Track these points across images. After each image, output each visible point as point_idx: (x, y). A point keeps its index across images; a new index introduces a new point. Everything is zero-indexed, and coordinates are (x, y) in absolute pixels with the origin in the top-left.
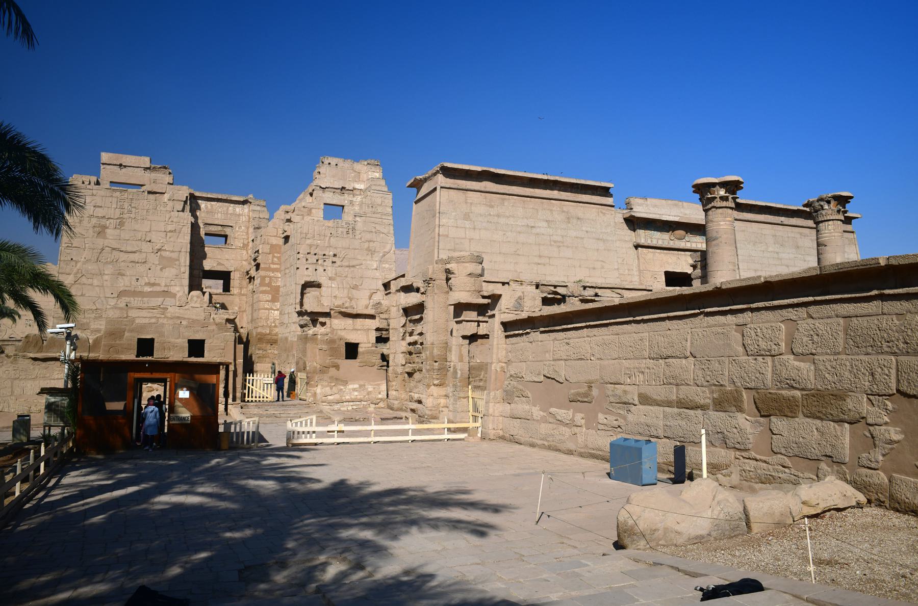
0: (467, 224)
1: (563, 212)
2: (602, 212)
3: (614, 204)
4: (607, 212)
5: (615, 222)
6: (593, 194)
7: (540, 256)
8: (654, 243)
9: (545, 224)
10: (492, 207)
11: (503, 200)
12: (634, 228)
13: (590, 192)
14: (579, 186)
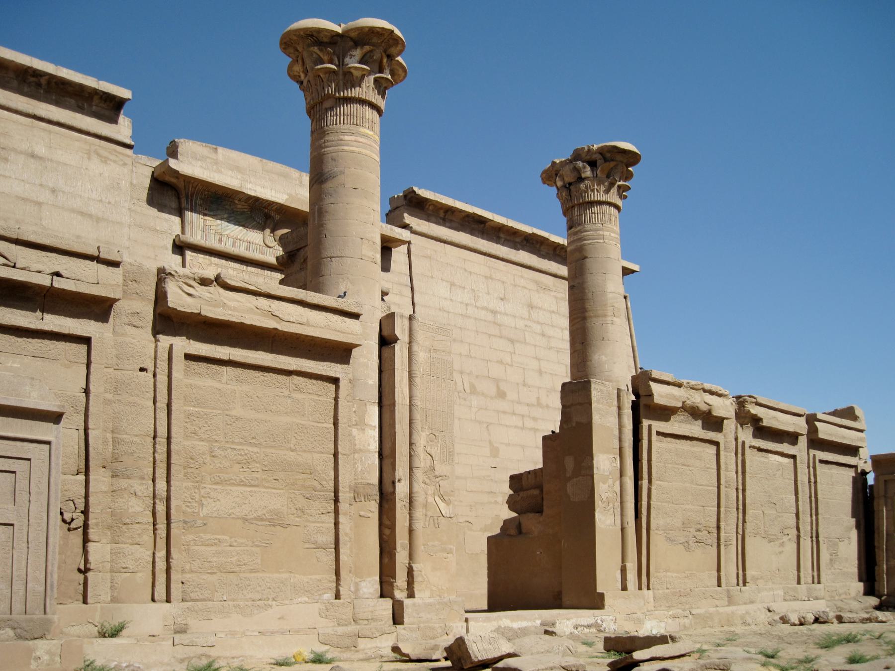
2: (98, 154)
3: (133, 143)
4: (112, 157)
5: (131, 184)
6: (80, 109)
8: (227, 247)
12: (180, 203)
13: (73, 102)
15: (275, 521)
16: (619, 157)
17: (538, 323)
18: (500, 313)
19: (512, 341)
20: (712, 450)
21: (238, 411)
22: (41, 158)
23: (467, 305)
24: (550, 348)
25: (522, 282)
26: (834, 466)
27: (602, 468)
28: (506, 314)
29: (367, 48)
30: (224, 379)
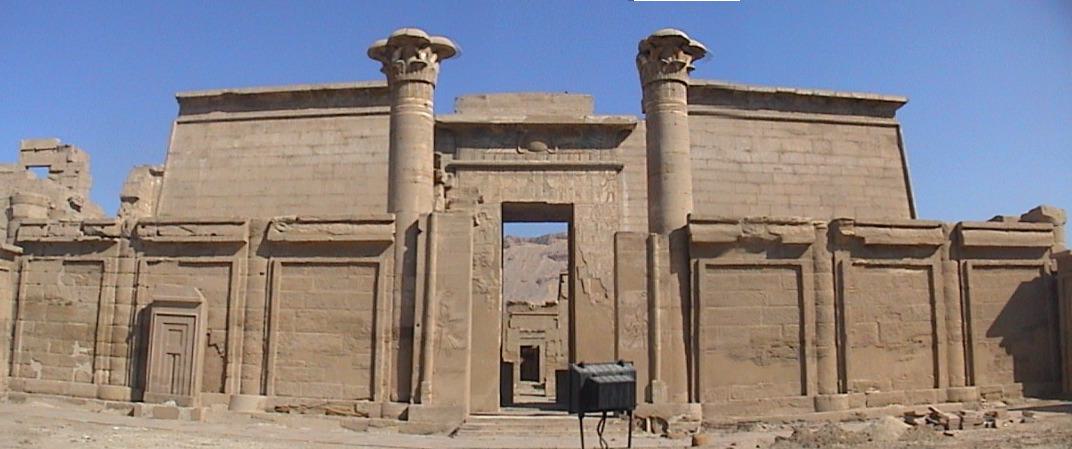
0: (203, 162)
1: (340, 130)
7: (296, 195)
9: (307, 151)
10: (238, 137)
11: (253, 127)
14: (367, 91)
15: (334, 352)
16: (664, 42)
17: (789, 164)
18: (746, 163)
19: (758, 184)
20: (793, 274)
21: (313, 290)
22: (366, 137)
23: (707, 160)
24: (802, 184)
25: (774, 133)
26: (1003, 270)
27: (628, 301)
28: (752, 163)
29: (400, 49)
30: (306, 273)
